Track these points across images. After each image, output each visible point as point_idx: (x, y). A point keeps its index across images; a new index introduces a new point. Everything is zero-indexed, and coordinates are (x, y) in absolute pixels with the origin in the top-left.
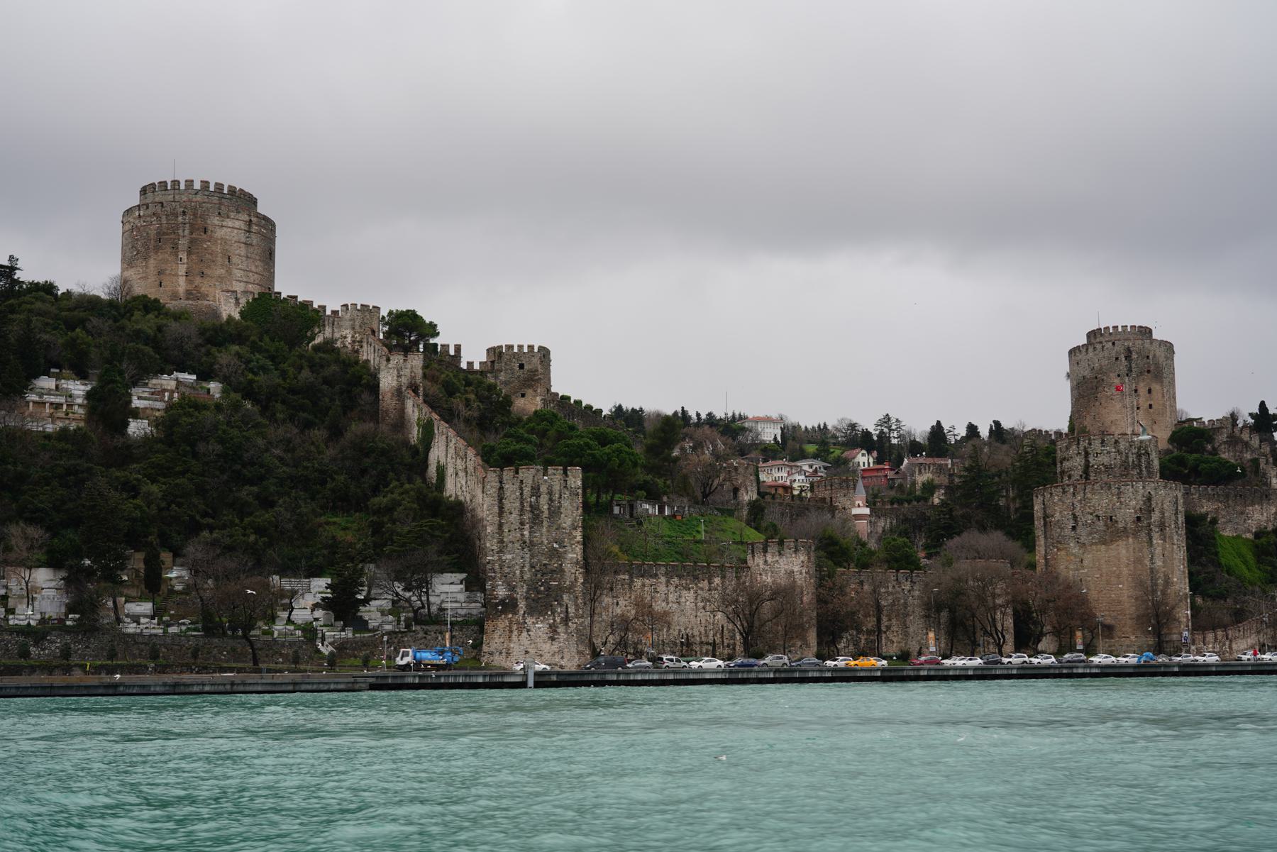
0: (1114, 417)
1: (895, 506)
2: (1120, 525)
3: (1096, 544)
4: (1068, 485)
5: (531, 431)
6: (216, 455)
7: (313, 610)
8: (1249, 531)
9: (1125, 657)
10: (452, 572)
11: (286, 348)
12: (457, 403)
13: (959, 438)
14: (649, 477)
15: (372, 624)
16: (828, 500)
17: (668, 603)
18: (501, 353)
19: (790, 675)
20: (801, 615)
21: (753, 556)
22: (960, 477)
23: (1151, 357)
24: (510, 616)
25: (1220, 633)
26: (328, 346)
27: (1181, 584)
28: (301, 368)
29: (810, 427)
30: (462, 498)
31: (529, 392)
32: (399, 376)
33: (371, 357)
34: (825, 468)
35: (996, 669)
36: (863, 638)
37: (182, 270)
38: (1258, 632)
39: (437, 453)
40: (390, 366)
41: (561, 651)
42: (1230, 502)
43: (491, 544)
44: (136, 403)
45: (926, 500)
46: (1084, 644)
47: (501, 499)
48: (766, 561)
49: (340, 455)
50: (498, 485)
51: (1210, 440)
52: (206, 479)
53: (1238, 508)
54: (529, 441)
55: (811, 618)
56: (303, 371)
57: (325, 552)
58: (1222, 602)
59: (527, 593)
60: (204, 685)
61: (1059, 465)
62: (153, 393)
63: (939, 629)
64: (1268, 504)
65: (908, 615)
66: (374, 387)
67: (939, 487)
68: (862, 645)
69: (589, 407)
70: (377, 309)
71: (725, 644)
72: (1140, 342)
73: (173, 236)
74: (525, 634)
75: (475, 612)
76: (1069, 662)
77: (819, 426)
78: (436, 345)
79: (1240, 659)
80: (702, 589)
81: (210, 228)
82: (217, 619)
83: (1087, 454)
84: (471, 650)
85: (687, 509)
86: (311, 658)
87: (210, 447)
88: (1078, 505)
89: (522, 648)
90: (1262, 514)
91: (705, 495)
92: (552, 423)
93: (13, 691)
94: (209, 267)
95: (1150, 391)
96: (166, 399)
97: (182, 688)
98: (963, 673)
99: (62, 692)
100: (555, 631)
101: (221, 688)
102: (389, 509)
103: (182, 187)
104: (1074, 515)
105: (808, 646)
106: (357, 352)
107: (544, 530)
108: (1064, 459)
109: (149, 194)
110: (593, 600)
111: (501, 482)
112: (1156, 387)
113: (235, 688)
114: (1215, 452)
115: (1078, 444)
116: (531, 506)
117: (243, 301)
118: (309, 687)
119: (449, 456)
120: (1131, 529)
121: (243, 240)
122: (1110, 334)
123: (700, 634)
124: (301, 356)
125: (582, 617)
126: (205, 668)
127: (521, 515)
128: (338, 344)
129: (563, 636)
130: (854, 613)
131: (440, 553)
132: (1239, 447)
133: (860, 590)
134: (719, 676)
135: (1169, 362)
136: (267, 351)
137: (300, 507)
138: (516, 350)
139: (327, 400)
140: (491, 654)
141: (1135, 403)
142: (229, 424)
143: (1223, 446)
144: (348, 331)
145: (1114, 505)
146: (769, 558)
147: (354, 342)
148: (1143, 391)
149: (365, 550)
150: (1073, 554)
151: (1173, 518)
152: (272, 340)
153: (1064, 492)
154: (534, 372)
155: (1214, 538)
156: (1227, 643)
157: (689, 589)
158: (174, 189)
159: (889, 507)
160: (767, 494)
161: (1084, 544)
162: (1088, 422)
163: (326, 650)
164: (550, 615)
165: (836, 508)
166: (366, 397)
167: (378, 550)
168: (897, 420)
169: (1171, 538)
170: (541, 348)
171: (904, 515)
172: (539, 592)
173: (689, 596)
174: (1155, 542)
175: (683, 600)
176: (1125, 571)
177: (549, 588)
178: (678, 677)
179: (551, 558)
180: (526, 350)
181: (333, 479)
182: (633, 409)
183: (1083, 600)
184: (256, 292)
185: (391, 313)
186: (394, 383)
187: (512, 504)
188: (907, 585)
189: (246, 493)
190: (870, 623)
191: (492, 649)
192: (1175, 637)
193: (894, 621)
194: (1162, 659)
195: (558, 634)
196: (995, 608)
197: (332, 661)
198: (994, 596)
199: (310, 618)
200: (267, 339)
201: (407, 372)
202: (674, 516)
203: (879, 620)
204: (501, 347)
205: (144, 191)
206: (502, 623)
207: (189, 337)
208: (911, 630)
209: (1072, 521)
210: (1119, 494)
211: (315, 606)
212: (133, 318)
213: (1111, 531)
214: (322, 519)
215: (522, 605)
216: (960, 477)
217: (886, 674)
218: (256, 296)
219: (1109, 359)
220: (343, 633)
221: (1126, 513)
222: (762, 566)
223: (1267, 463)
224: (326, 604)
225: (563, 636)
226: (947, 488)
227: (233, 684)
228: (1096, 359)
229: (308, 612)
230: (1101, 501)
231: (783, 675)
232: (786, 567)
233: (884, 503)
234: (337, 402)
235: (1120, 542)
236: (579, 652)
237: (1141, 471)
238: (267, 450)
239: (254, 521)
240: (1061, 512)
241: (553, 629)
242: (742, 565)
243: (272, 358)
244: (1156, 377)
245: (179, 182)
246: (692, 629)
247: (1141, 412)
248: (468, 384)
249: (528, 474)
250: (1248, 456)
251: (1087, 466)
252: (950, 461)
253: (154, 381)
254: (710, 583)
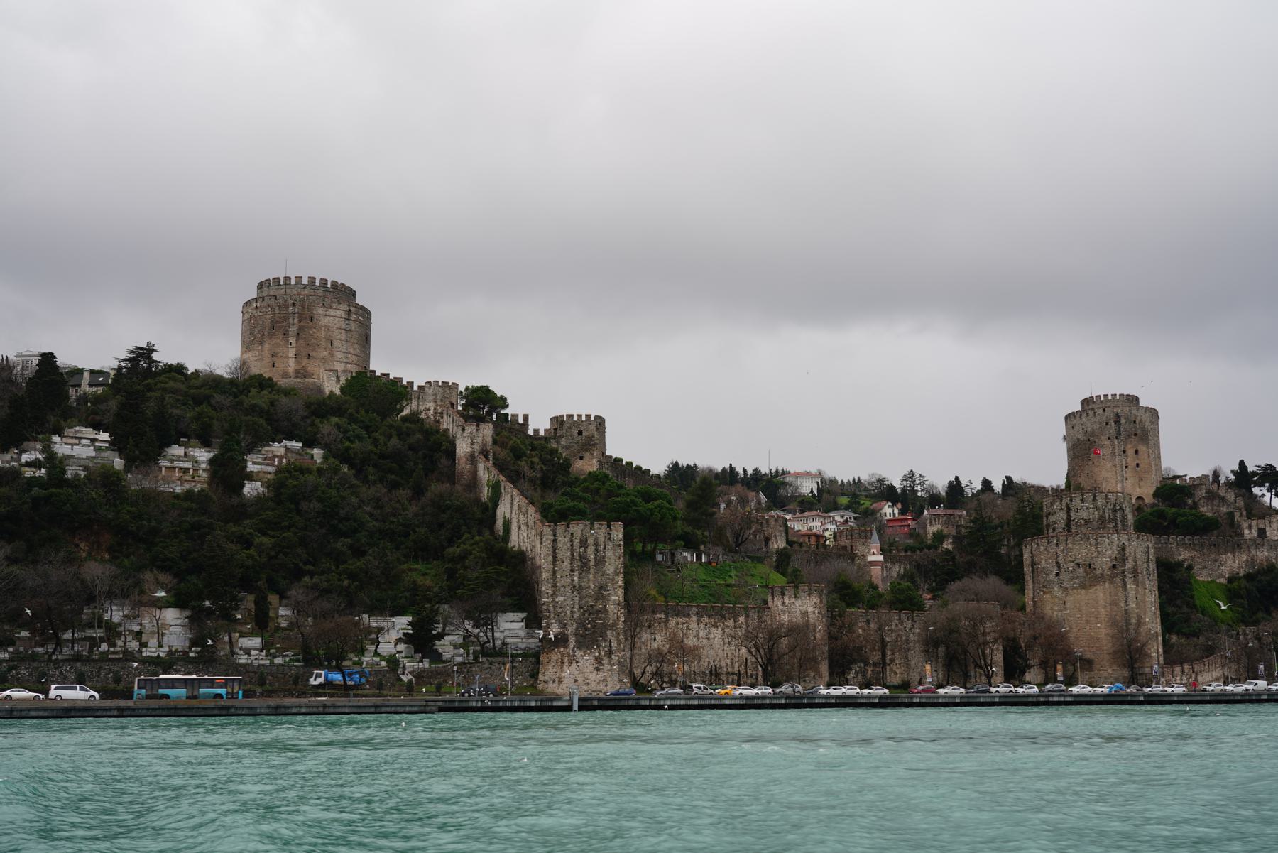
0: (1104, 474)
1: (909, 553)
2: (1098, 572)
3: (1076, 588)
4: (1052, 537)
5: (586, 490)
6: (317, 512)
7: (396, 644)
8: (1223, 577)
9: (1101, 687)
10: (514, 612)
11: (379, 419)
12: (523, 465)
13: (975, 491)
14: (689, 529)
15: (446, 656)
16: (849, 548)
17: (698, 639)
18: (562, 421)
19: (799, 701)
20: (814, 649)
21: (773, 599)
22: (966, 528)
23: (1137, 422)
24: (562, 649)
25: (1187, 667)
26: (414, 418)
27: (1153, 623)
28: (390, 436)
29: (845, 481)
30: (524, 548)
31: (587, 455)
32: (472, 443)
33: (450, 427)
34: (855, 518)
35: (980, 697)
36: (870, 669)
37: (292, 352)
38: (1223, 666)
39: (503, 510)
40: (465, 435)
41: (605, 680)
42: (1205, 551)
43: (546, 588)
44: (251, 467)
45: (936, 548)
46: (1064, 675)
47: (554, 550)
48: (784, 603)
49: (421, 512)
50: (552, 537)
51: (1191, 495)
52: (308, 533)
53: (1213, 556)
54: (583, 499)
55: (823, 653)
56: (392, 439)
57: (407, 594)
58: (1195, 639)
59: (577, 629)
60: (301, 707)
61: (1045, 519)
62: (265, 459)
63: (937, 662)
64: (1240, 552)
65: (909, 650)
66: (451, 453)
67: (948, 536)
68: (869, 676)
69: (639, 468)
70: (455, 385)
71: (749, 674)
72: (1128, 409)
73: (284, 324)
74: (574, 665)
75: (533, 646)
76: (1050, 691)
77: (854, 480)
78: (507, 415)
79: (1205, 690)
80: (728, 627)
81: (315, 317)
82: (315, 652)
83: (1069, 510)
84: (529, 678)
85: (721, 556)
86: (393, 685)
87: (312, 506)
88: (1061, 555)
89: (572, 677)
90: (1234, 562)
91: (738, 545)
92: (604, 483)
93: (144, 712)
94: (314, 350)
95: (1137, 452)
96: (276, 463)
97: (283, 710)
98: (951, 700)
99: (184, 713)
100: (600, 663)
101: (315, 710)
102: (462, 557)
103: (293, 282)
104: (1057, 563)
105: (821, 676)
106: (438, 422)
107: (591, 576)
108: (1049, 514)
109: (265, 289)
110: (633, 636)
111: (555, 535)
112: (1142, 448)
113: (327, 710)
114: (1195, 506)
115: (1061, 501)
116: (580, 556)
117: (343, 379)
118: (388, 709)
119: (514, 512)
120: (1107, 575)
121: (343, 326)
122: (1101, 401)
123: (727, 665)
124: (391, 426)
125: (623, 651)
126: (304, 693)
127: (571, 563)
128: (423, 416)
129: (607, 667)
130: (861, 648)
131: (503, 595)
132: (1216, 502)
133: (866, 628)
134: (738, 702)
135: (1154, 426)
136: (362, 421)
137: (387, 556)
138: (575, 419)
139: (412, 464)
140: (546, 682)
142: (329, 486)
143: (1202, 501)
144: (430, 404)
145: (1092, 554)
146: (787, 600)
147: (436, 413)
148: (1130, 452)
149: (441, 592)
150: (1057, 597)
151: (1145, 565)
152: (367, 412)
153: (1049, 543)
154: (591, 438)
155: (1190, 583)
156: (1193, 676)
157: (717, 627)
158: (286, 284)
159: (903, 554)
160: (795, 542)
161: (1067, 588)
162: (1082, 480)
163: (405, 678)
164: (595, 649)
165: (856, 555)
166: (444, 461)
167: (452, 593)
168: (920, 475)
169: (1143, 583)
170: (597, 417)
171: (916, 562)
172: (587, 629)
173: (717, 633)
174: (1129, 586)
175: (712, 636)
176: (1103, 612)
177: (595, 626)
178: (702, 702)
179: (596, 600)
180: (584, 419)
181: (415, 532)
182: (688, 465)
183: (1063, 637)
184: (354, 371)
185: (467, 388)
186: (468, 450)
187: (563, 554)
188: (908, 625)
189: (341, 544)
190: (875, 657)
191: (546, 678)
192: (1147, 670)
193: (897, 655)
194: (1132, 689)
195: (603, 665)
196: (986, 643)
197: (410, 688)
198: (984, 634)
199: (394, 651)
200: (363, 412)
201: (479, 440)
202: (710, 563)
203: (884, 655)
204: (563, 416)
205: (260, 286)
206: (555, 656)
207: (297, 411)
208: (913, 663)
209: (1056, 568)
210: (1097, 545)
211: (398, 641)
212: (250, 394)
213: (1090, 577)
214: (405, 566)
215: (572, 640)
216: (966, 528)
217: (884, 701)
218: (354, 374)
219: (1100, 423)
220: (421, 664)
221: (1102, 562)
222: (780, 607)
223: (1241, 515)
224: (407, 639)
225: (607, 667)
226: (955, 537)
227: (325, 706)
228: (1089, 424)
229: (392, 645)
230: (1081, 551)
231: (793, 702)
232: (801, 608)
233: (898, 551)
234: (420, 466)
235: (1098, 587)
236: (620, 681)
237: (1116, 524)
238: (360, 507)
239: (348, 569)
240: (1046, 560)
241: (598, 660)
242: (764, 607)
243: (367, 428)
244: (1142, 439)
245: (290, 278)
246: (720, 661)
247: (1129, 470)
248: (534, 449)
249: (577, 528)
250: (1224, 509)
251: (1069, 521)
252: (965, 512)
253: (266, 448)
254: (735, 622)
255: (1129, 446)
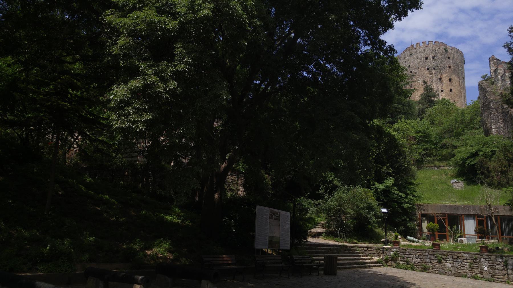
95: (450, 80)
141: (440, 87)
148: (445, 79)
219: (421, 59)
255: (444, 75)
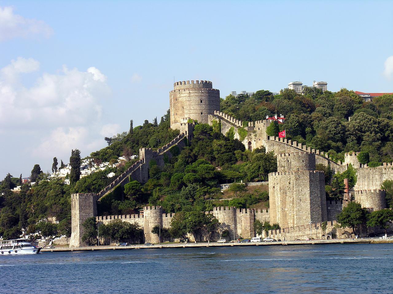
121: (188, 100)
156: (284, 234)
